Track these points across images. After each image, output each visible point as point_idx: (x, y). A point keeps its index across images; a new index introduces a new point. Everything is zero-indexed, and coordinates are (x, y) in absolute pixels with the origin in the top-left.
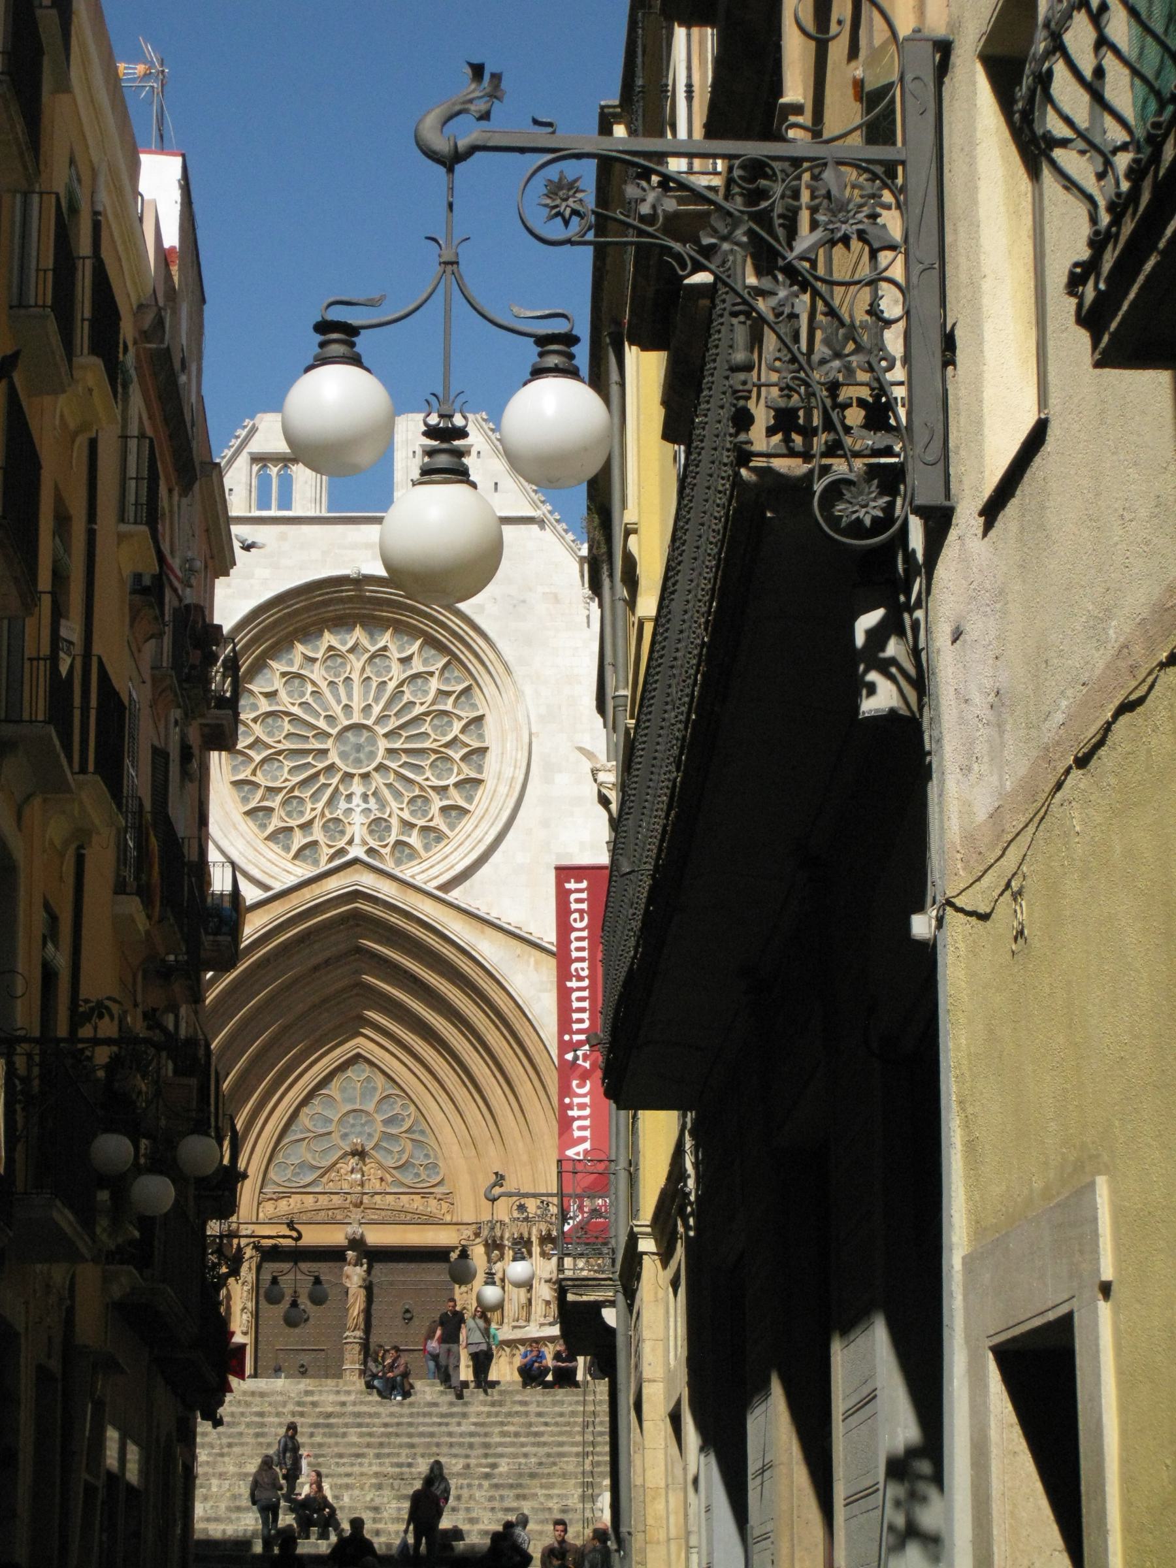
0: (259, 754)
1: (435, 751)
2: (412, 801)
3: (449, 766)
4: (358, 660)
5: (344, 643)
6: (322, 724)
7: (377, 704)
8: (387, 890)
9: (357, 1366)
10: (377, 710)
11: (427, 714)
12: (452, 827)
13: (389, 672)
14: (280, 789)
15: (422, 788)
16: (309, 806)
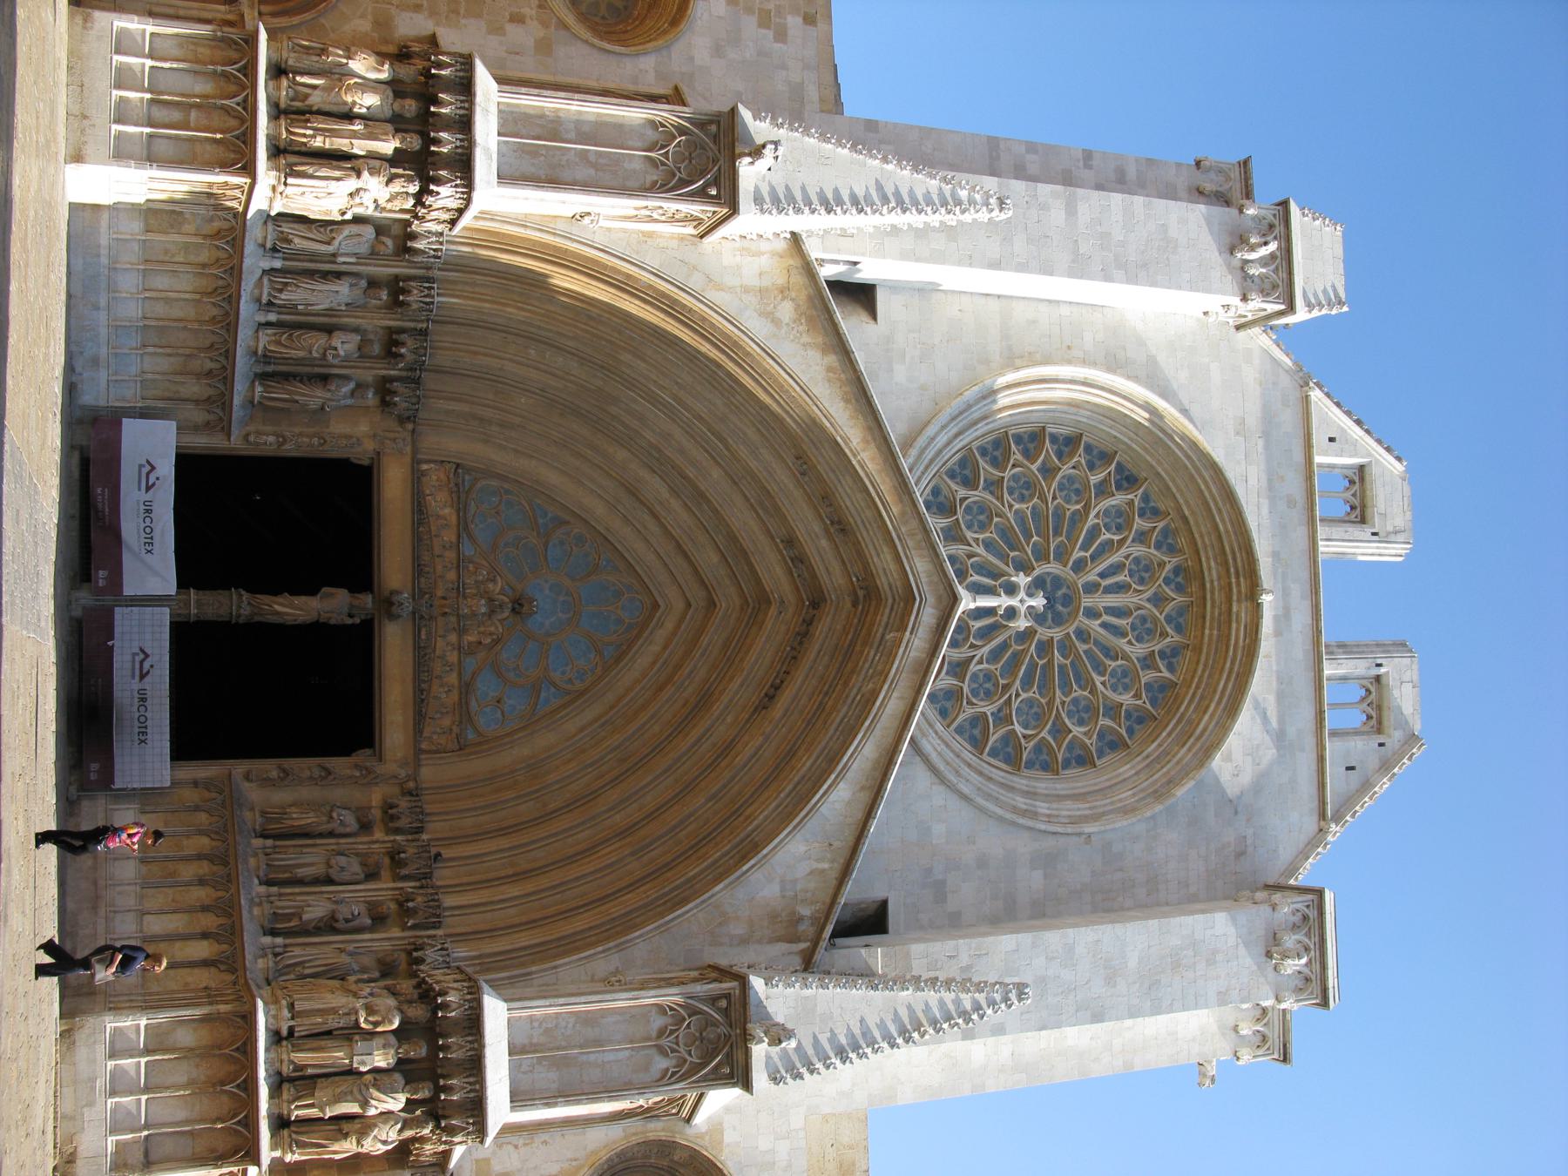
0: (1038, 470)
1: (1051, 703)
2: (988, 676)
3: (1033, 723)
4: (1149, 600)
5: (1167, 581)
6: (1077, 554)
7: (1100, 625)
8: (915, 643)
9: (194, 611)
10: (1095, 624)
11: (1093, 691)
12: (959, 730)
13: (1138, 641)
14: (1001, 499)
15: (1006, 687)
16: (981, 536)
